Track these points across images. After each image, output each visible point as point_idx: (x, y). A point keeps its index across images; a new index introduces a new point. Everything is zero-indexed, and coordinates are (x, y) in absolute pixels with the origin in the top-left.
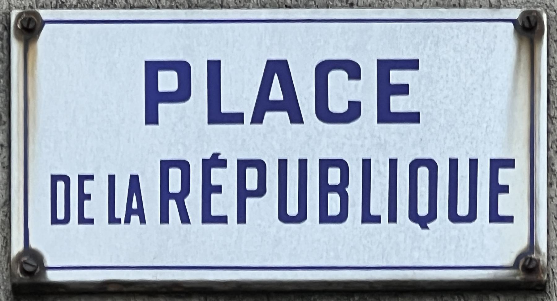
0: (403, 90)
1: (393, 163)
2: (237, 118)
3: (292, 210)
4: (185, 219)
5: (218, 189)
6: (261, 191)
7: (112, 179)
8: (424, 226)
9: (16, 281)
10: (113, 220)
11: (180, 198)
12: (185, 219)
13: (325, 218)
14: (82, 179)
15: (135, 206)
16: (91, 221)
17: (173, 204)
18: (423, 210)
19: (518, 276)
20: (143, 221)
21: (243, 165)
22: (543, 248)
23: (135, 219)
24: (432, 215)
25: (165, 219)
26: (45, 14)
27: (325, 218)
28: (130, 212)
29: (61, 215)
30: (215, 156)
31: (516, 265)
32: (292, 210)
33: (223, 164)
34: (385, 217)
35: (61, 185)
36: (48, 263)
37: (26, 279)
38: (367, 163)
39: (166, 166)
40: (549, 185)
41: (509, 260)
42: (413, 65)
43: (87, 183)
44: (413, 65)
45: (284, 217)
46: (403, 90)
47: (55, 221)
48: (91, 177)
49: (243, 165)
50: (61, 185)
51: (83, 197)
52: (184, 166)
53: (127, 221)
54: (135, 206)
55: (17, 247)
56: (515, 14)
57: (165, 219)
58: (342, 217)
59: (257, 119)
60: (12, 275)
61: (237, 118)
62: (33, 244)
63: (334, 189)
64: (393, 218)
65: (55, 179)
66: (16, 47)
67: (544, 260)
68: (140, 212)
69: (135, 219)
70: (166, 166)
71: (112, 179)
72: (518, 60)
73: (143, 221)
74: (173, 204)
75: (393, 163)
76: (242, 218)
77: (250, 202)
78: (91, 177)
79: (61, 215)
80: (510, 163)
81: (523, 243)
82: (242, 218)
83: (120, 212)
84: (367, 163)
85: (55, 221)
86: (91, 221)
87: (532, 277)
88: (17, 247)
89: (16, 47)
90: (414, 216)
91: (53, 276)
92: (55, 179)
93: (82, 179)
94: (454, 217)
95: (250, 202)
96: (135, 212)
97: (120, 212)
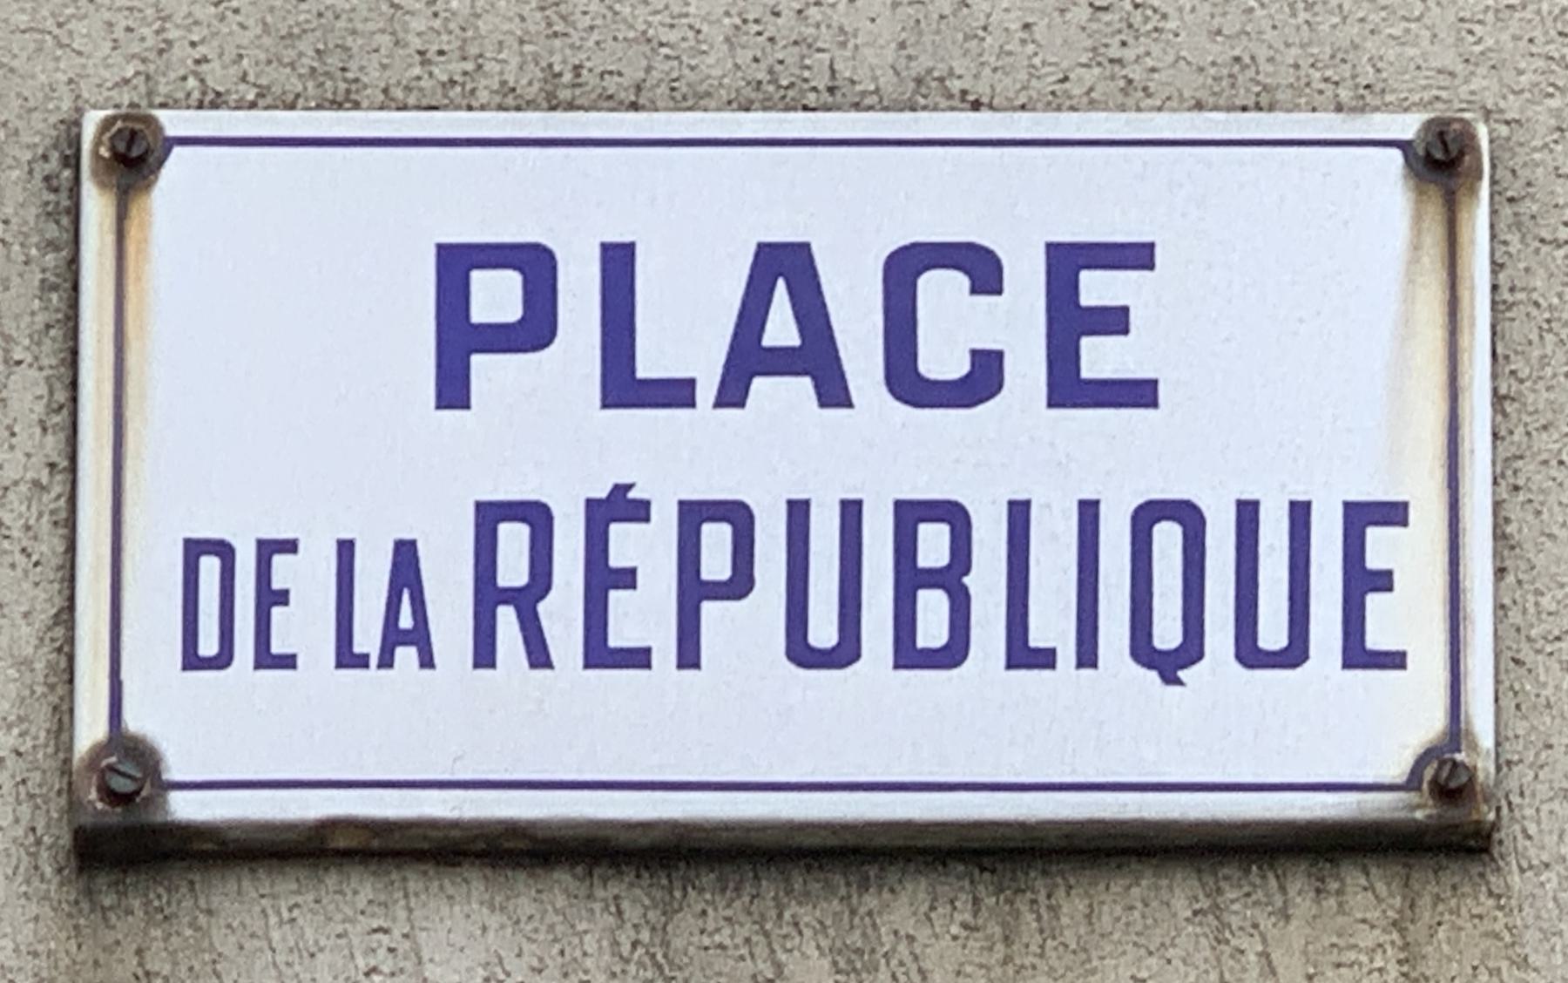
0: (1115, 321)
1: (1089, 512)
2: (678, 393)
3: (823, 631)
4: (539, 655)
5: (627, 578)
6: (739, 585)
7: (346, 549)
8: (1170, 679)
9: (86, 820)
10: (347, 658)
11: (527, 600)
12: (539, 655)
13: (908, 655)
14: (268, 549)
15: (406, 621)
16: (288, 662)
17: (507, 617)
18: (1167, 633)
19: (1420, 810)
20: (427, 661)
21: (693, 515)
22: (1486, 741)
23: (406, 655)
24: (1192, 649)
25: (485, 655)
26: (173, 122)
27: (908, 655)
28: (392, 638)
29: (208, 645)
30: (621, 490)
31: (1412, 782)
32: (823, 631)
33: (640, 512)
34: (1067, 653)
35: (210, 566)
36: (175, 770)
37: (115, 816)
38: (1019, 514)
39: (489, 516)
40: (1500, 572)
41: (1396, 768)
42: (1139, 256)
43: (278, 560)
44: (1139, 256)
45: (802, 653)
46: (1115, 321)
47: (192, 661)
48: (290, 547)
49: (693, 515)
50: (210, 566)
51: (270, 598)
52: (537, 517)
53: (386, 661)
54: (406, 621)
55: (90, 730)
56: (1408, 126)
57: (485, 655)
58: (953, 653)
59: (732, 394)
60: (74, 804)
61: (678, 393)
62: (134, 722)
63: (933, 578)
64: (1087, 656)
65: (194, 549)
66: (96, 205)
67: (1485, 767)
68: (420, 637)
69: (406, 655)
70: (489, 516)
71: (346, 549)
72: (1416, 247)
73: (427, 661)
74: (507, 617)
75: (1089, 512)
76: (689, 656)
77: (711, 611)
78: (290, 547)
79: (208, 645)
80: (1394, 514)
81: (1431, 724)
82: (689, 656)
83: (368, 638)
84: (1019, 514)
85: (192, 661)
86: (288, 662)
87: (1454, 814)
88: (90, 730)
89: (96, 205)
90: (1143, 650)
91: (185, 808)
92: (194, 549)
93: (268, 549)
94: (1250, 654)
95: (709, 609)
96: (406, 638)
97: (368, 638)
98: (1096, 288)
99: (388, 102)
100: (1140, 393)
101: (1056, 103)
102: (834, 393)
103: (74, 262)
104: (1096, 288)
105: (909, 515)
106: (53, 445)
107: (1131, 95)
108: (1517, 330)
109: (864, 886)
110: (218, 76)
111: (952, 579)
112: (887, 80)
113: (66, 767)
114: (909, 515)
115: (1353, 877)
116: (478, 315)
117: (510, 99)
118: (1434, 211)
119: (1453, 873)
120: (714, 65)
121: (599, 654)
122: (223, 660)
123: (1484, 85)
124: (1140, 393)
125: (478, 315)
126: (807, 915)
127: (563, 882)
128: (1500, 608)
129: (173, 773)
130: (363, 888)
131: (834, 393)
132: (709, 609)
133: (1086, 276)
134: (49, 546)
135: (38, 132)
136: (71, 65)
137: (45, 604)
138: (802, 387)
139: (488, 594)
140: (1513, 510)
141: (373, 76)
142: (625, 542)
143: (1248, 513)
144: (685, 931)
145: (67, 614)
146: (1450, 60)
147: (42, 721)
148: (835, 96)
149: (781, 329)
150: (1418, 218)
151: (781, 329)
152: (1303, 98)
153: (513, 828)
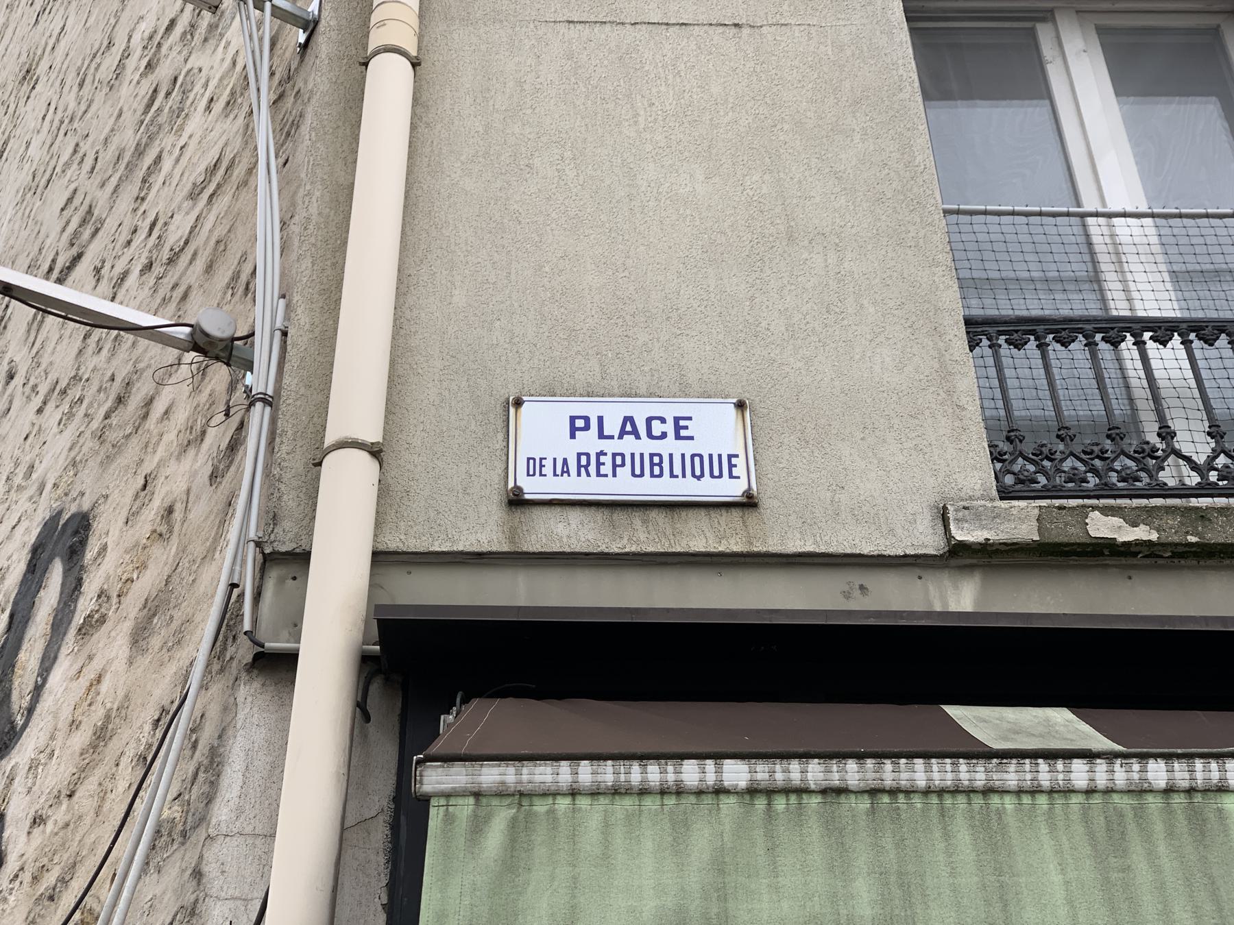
0: (686, 428)
1: (683, 455)
2: (612, 437)
3: (638, 472)
4: (588, 475)
5: (604, 464)
6: (623, 465)
7: (555, 460)
8: (699, 480)
9: (510, 498)
10: (555, 475)
11: (586, 467)
12: (588, 475)
13: (652, 475)
14: (541, 459)
15: (565, 470)
16: (545, 475)
17: (583, 469)
18: (698, 473)
19: (745, 500)
20: (569, 475)
21: (614, 455)
22: (755, 489)
23: (565, 475)
24: (702, 475)
25: (579, 474)
26: (525, 398)
27: (652, 475)
28: (563, 472)
29: (531, 473)
30: (602, 451)
31: (743, 496)
32: (638, 472)
33: (606, 454)
34: (680, 475)
35: (531, 461)
36: (525, 491)
37: (515, 498)
38: (671, 456)
39: (579, 455)
40: (755, 465)
41: (740, 493)
42: (690, 418)
43: (543, 461)
44: (690, 418)
45: (634, 475)
46: (686, 428)
47: (528, 475)
48: (545, 459)
49: (614, 455)
50: (531, 461)
51: (542, 466)
52: (588, 455)
53: (562, 475)
54: (565, 470)
55: (511, 485)
56: (735, 400)
57: (579, 474)
58: (661, 475)
59: (621, 437)
60: (508, 496)
61: (612, 437)
62: (518, 484)
63: (656, 464)
64: (684, 476)
65: (529, 459)
66: (512, 410)
67: (755, 494)
68: (568, 472)
69: (565, 475)
70: (579, 455)
71: (555, 460)
72: (737, 417)
73: (569, 475)
74: (583, 469)
75: (683, 455)
76: (614, 475)
77: (618, 469)
78: (545, 459)
79: (531, 473)
80: (737, 456)
81: (745, 487)
82: (614, 475)
83: (559, 471)
84: (671, 456)
85: (528, 475)
86: (545, 475)
87: (750, 501)
88: (511, 485)
89: (512, 410)
90: (693, 475)
91: (527, 497)
92: (529, 459)
93: (541, 459)
94: (712, 476)
95: (617, 468)
96: (565, 472)
97: (559, 471)
98: (682, 423)
99: (561, 396)
100: (691, 438)
101: (674, 397)
102: (638, 437)
103: (508, 418)
104: (682, 423)
105: (652, 456)
106: (505, 444)
107: (686, 396)
108: (756, 429)
109: (647, 510)
110: (532, 392)
111: (660, 464)
112: (645, 393)
113: (507, 490)
114: (652, 456)
115: (733, 510)
116: (577, 426)
117: (581, 395)
118: (740, 412)
119: (751, 510)
120: (616, 391)
121: (599, 474)
122: (534, 475)
123: (747, 395)
124: (691, 438)
125: (577, 426)
126: (637, 514)
127: (593, 509)
128: (756, 470)
129: (525, 492)
130: (558, 509)
131: (638, 437)
132: (617, 468)
133: (681, 431)
134: (504, 458)
135: (503, 399)
136: (507, 390)
137: (503, 467)
138: (632, 437)
139: (579, 466)
140: (757, 455)
141: (558, 392)
142: (602, 459)
143: (711, 456)
144: (615, 516)
145: (507, 468)
146: (741, 391)
147: (503, 483)
148: (636, 395)
149: (629, 428)
150: (737, 414)
151: (629, 428)
152: (715, 396)
153: (585, 501)
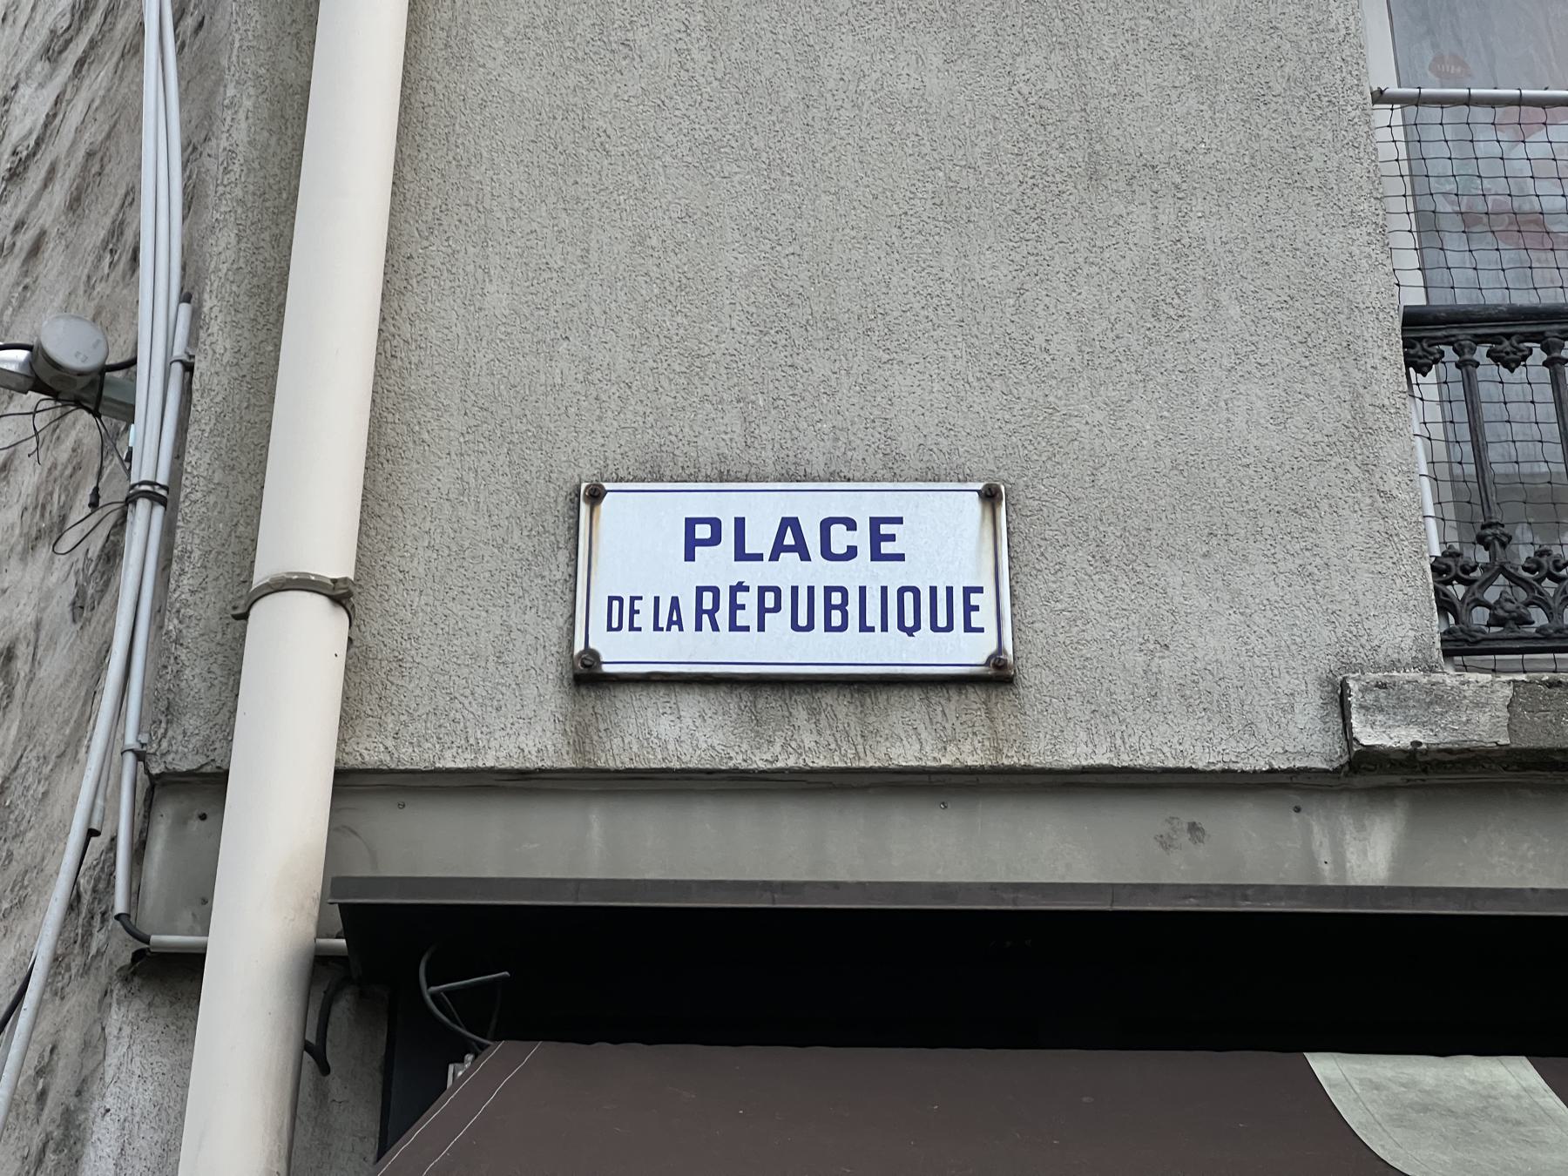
0: (892, 538)
1: (884, 590)
2: (758, 557)
3: (802, 621)
4: (715, 627)
5: (743, 607)
7: (657, 599)
8: (911, 635)
9: (577, 671)
10: (657, 628)
11: (712, 614)
12: (715, 627)
13: (829, 627)
14: (633, 599)
15: (675, 618)
16: (639, 629)
17: (705, 617)
18: (909, 622)
19: (990, 672)
20: (681, 629)
21: (762, 591)
22: (1010, 652)
23: (675, 628)
24: (917, 626)
25: (699, 627)
26: (607, 486)
27: (829, 627)
28: (670, 623)
29: (615, 624)
30: (740, 583)
31: (987, 664)
32: (802, 621)
33: (747, 589)
34: (878, 627)
35: (616, 604)
36: (603, 659)
37: (586, 671)
38: (863, 590)
39: (700, 591)
40: (1013, 605)
41: (983, 660)
42: (899, 521)
44: (899, 521)
45: (795, 626)
46: (892, 538)
47: (610, 628)
48: (640, 598)
49: (762, 591)
50: (616, 604)
51: (633, 612)
52: (715, 591)
53: (669, 629)
54: (675, 618)
55: (579, 647)
56: (980, 486)
57: (699, 627)
59: (774, 557)
60: (574, 667)
61: (758, 557)
62: (592, 645)
63: (836, 607)
64: (884, 628)
65: (611, 599)
66: (584, 508)
67: (1010, 659)
68: (679, 623)
69: (675, 628)
70: (700, 591)
71: (657, 599)
73: (681, 629)
74: (705, 617)
75: (884, 590)
76: (761, 628)
78: (640, 598)
79: (615, 624)
80: (979, 590)
81: (993, 647)
82: (761, 628)
83: (663, 623)
84: (863, 590)
86: (639, 629)
87: (1000, 673)
88: (579, 647)
89: (584, 508)
90: (901, 626)
91: (606, 669)
92: (611, 599)
93: (633, 599)
94: (935, 627)
95: (767, 616)
96: (675, 623)
97: (663, 623)
98: (885, 529)
99: (672, 480)
101: (872, 480)
102: (805, 556)
104: (885, 529)
105: (828, 591)
106: (570, 570)
107: (895, 478)
108: (1016, 539)
109: (817, 691)
110: (622, 473)
111: (843, 607)
112: (822, 474)
114: (828, 591)
116: (698, 536)
117: (708, 479)
120: (770, 469)
121: (733, 627)
123: (1003, 474)
125: (698, 536)
127: (722, 691)
128: (1013, 615)
131: (805, 556)
132: (767, 616)
134: (568, 597)
135: (568, 488)
136: (578, 470)
137: (567, 612)
139: (700, 611)
140: (1017, 587)
141: (668, 473)
142: (741, 598)
143: (933, 590)
145: (573, 615)
147: (565, 644)
148: (806, 478)
149: (789, 540)
151: (789, 540)
